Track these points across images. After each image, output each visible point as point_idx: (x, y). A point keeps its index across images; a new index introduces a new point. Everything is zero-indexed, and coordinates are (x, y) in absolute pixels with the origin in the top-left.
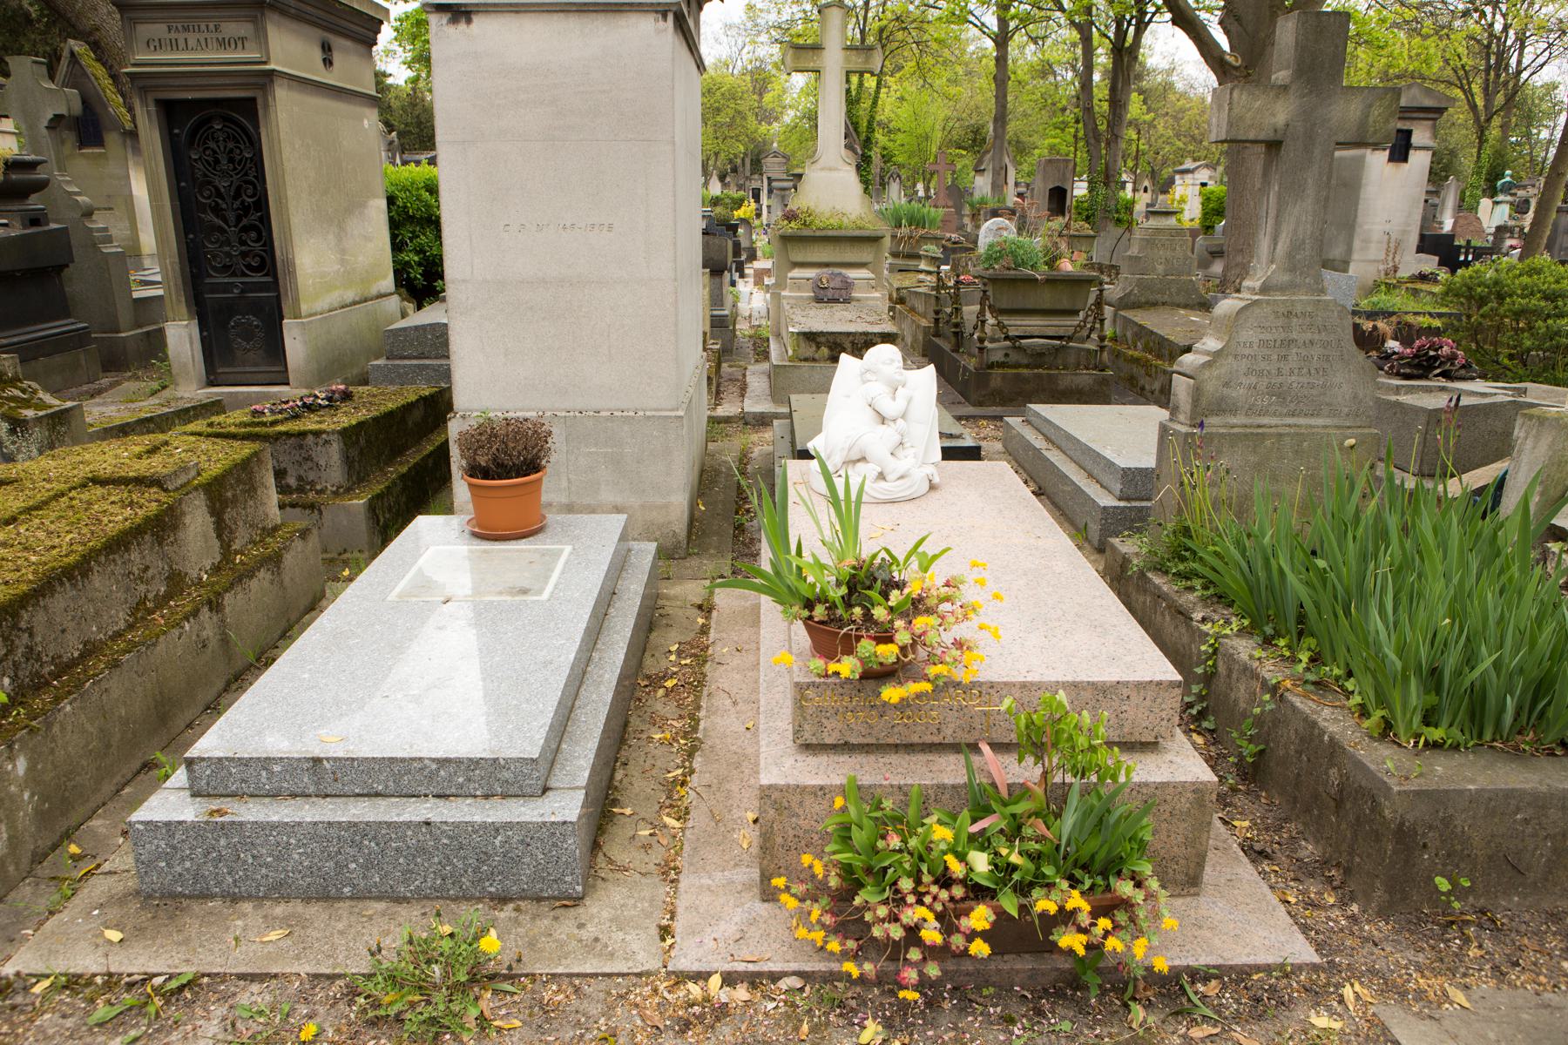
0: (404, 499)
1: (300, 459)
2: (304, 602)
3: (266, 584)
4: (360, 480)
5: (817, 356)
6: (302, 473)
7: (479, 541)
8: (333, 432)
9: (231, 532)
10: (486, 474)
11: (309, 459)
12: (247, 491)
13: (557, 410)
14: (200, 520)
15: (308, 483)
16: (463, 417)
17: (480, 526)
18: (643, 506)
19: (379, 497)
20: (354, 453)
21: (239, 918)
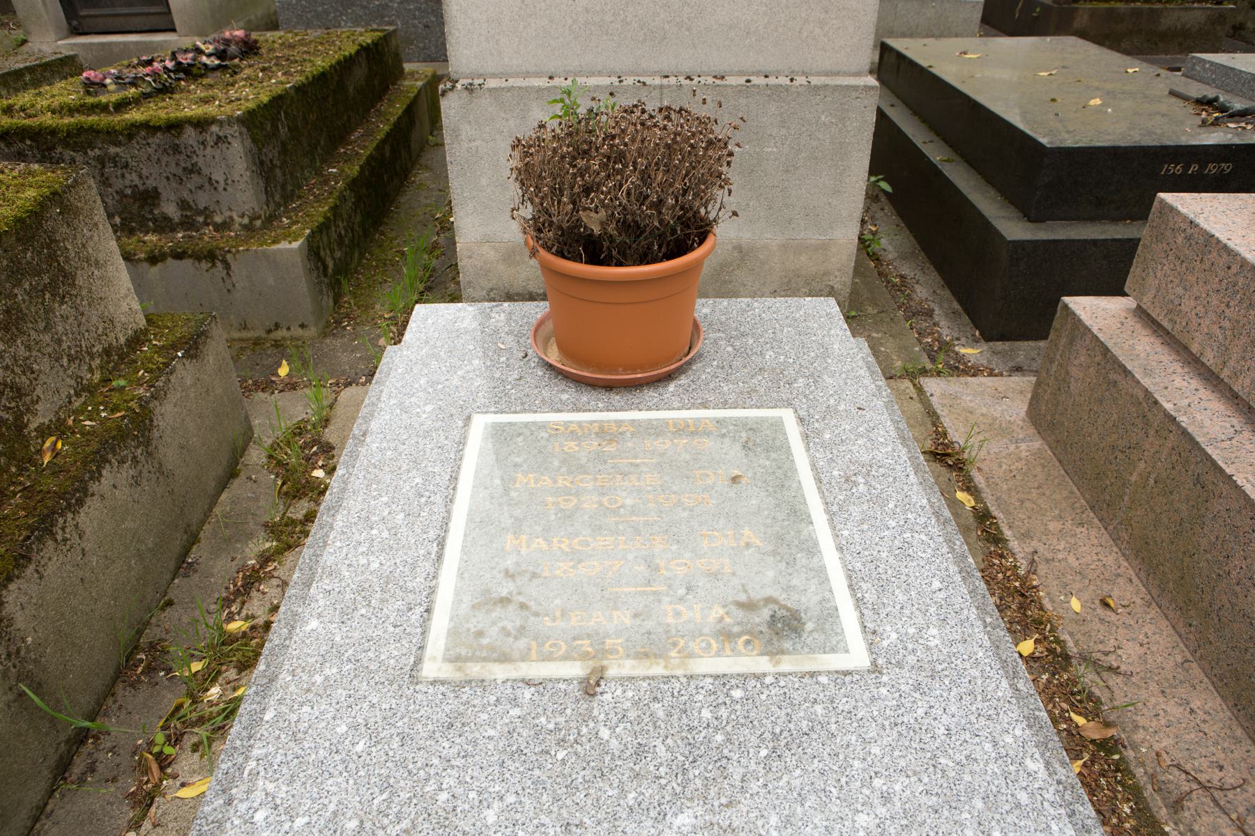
0: (358, 219)
1: (179, 171)
2: (219, 471)
4: (288, 198)
6: (185, 195)
7: (568, 394)
8: (230, 121)
10: (594, 251)
11: (193, 170)
13: (645, 74)
15: (200, 213)
16: (469, 89)
17: (564, 350)
18: (784, 247)
19: (323, 228)
20: (271, 152)
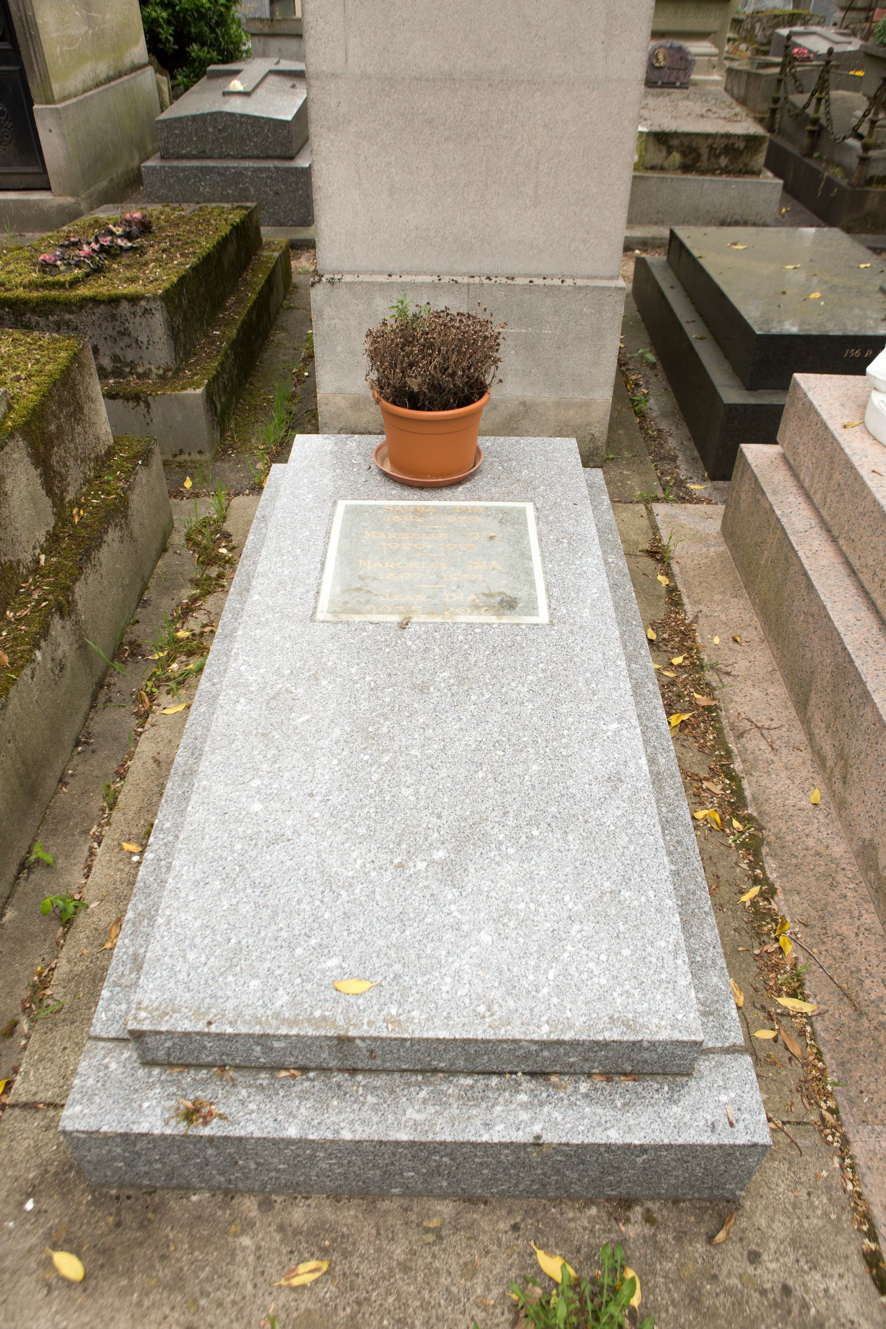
0: (236, 372)
1: (115, 334)
2: (156, 545)
3: (116, 545)
4: (188, 355)
5: (666, 164)
6: (118, 351)
7: (396, 490)
8: (155, 298)
9: (63, 479)
10: (414, 401)
11: (125, 333)
12: (73, 415)
13: (457, 274)
14: (24, 480)
15: (127, 365)
16: (331, 282)
17: (395, 464)
18: (558, 404)
19: (215, 380)
20: (178, 320)
21: (243, 1232)
